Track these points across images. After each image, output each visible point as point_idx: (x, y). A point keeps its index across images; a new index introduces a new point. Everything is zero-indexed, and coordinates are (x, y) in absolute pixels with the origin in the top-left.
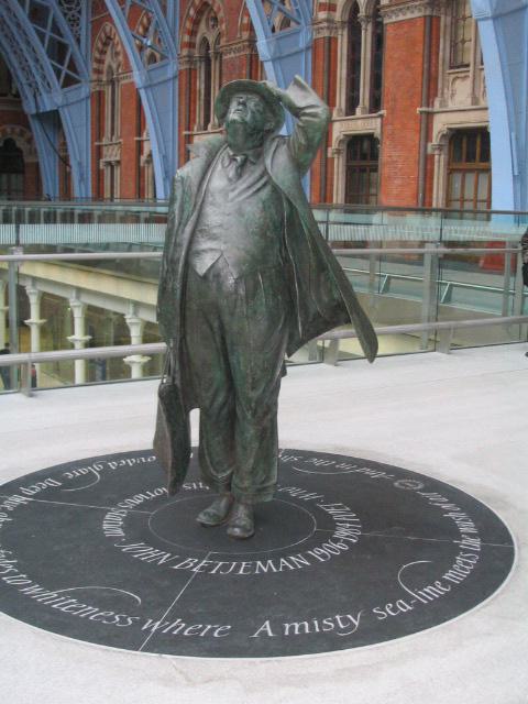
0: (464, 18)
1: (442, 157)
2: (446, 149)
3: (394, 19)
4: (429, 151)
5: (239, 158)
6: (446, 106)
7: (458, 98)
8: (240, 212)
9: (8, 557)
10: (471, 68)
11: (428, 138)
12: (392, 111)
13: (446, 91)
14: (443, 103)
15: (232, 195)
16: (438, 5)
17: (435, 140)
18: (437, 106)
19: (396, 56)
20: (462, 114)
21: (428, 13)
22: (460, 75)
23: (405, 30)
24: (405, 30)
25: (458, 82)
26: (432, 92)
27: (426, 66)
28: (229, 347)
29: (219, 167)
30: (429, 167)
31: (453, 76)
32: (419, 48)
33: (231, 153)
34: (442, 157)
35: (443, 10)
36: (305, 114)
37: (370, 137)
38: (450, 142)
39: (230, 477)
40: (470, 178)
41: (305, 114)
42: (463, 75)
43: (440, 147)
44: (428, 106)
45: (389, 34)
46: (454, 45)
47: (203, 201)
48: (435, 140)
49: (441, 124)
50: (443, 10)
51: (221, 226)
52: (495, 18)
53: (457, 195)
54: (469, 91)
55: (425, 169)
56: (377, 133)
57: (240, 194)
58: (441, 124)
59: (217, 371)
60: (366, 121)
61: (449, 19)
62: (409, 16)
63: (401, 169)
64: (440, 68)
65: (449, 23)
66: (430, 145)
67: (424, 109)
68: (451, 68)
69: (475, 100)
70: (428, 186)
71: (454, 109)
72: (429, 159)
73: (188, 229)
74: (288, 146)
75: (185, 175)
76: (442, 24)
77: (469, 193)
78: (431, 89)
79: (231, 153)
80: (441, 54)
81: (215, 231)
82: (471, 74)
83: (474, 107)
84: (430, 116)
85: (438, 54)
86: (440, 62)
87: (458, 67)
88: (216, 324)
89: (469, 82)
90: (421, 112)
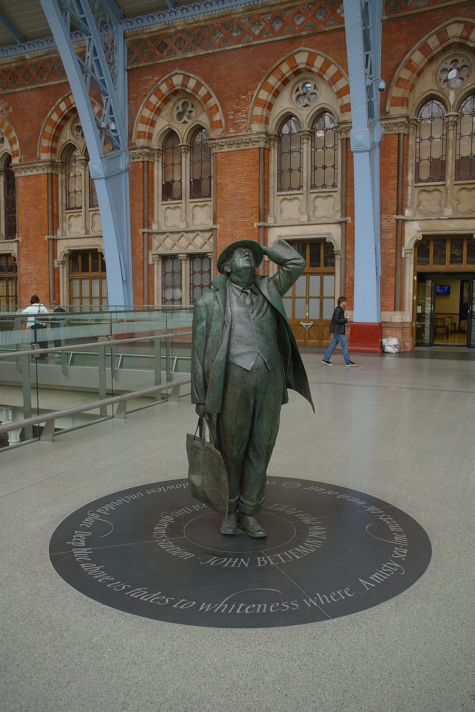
0: (75, 176)
1: (65, 269)
2: (67, 263)
3: (23, 174)
4: (56, 266)
5: (249, 291)
6: (66, 235)
7: (72, 229)
8: (260, 326)
9: (150, 592)
10: (83, 210)
11: (55, 256)
12: (26, 238)
13: (64, 224)
14: (63, 232)
15: (253, 316)
16: (56, 167)
17: (60, 258)
18: (59, 233)
19: (27, 199)
20: (79, 240)
21: (50, 171)
22: (74, 214)
23: (33, 182)
24: (31, 183)
25: (72, 218)
26: (55, 226)
27: (50, 207)
28: (257, 415)
29: (234, 298)
30: (56, 276)
31: (69, 215)
32: (44, 196)
33: (241, 288)
34: (65, 269)
35: (59, 170)
36: (293, 264)
37: (8, 255)
38: (69, 260)
39: (239, 500)
40: (86, 283)
41: (293, 264)
42: (76, 214)
43: (63, 263)
44: (53, 235)
45: (20, 184)
46: (68, 193)
47: (232, 321)
48: (60, 258)
49: (63, 247)
50: (59, 170)
51: (253, 336)
52: (106, 178)
53: (77, 294)
54: (84, 226)
55: (54, 278)
56: (15, 252)
57: (257, 314)
58: (63, 247)
59: (237, 431)
60: (4, 244)
61: (64, 176)
62: (35, 172)
63: (35, 279)
64: (60, 209)
65: (64, 180)
66: (56, 261)
67: (51, 237)
68: (67, 209)
69: (87, 232)
70: (56, 289)
71: (73, 234)
72: (56, 271)
73: (225, 340)
74: (274, 283)
75: (207, 303)
76: (59, 179)
77: (86, 293)
78: (54, 222)
79: (241, 288)
80: (60, 200)
81: (249, 340)
82: (83, 214)
83: (87, 236)
84: (55, 241)
85: (57, 199)
86: (60, 205)
87: (72, 209)
88: (252, 401)
89: (81, 219)
90: (48, 239)
